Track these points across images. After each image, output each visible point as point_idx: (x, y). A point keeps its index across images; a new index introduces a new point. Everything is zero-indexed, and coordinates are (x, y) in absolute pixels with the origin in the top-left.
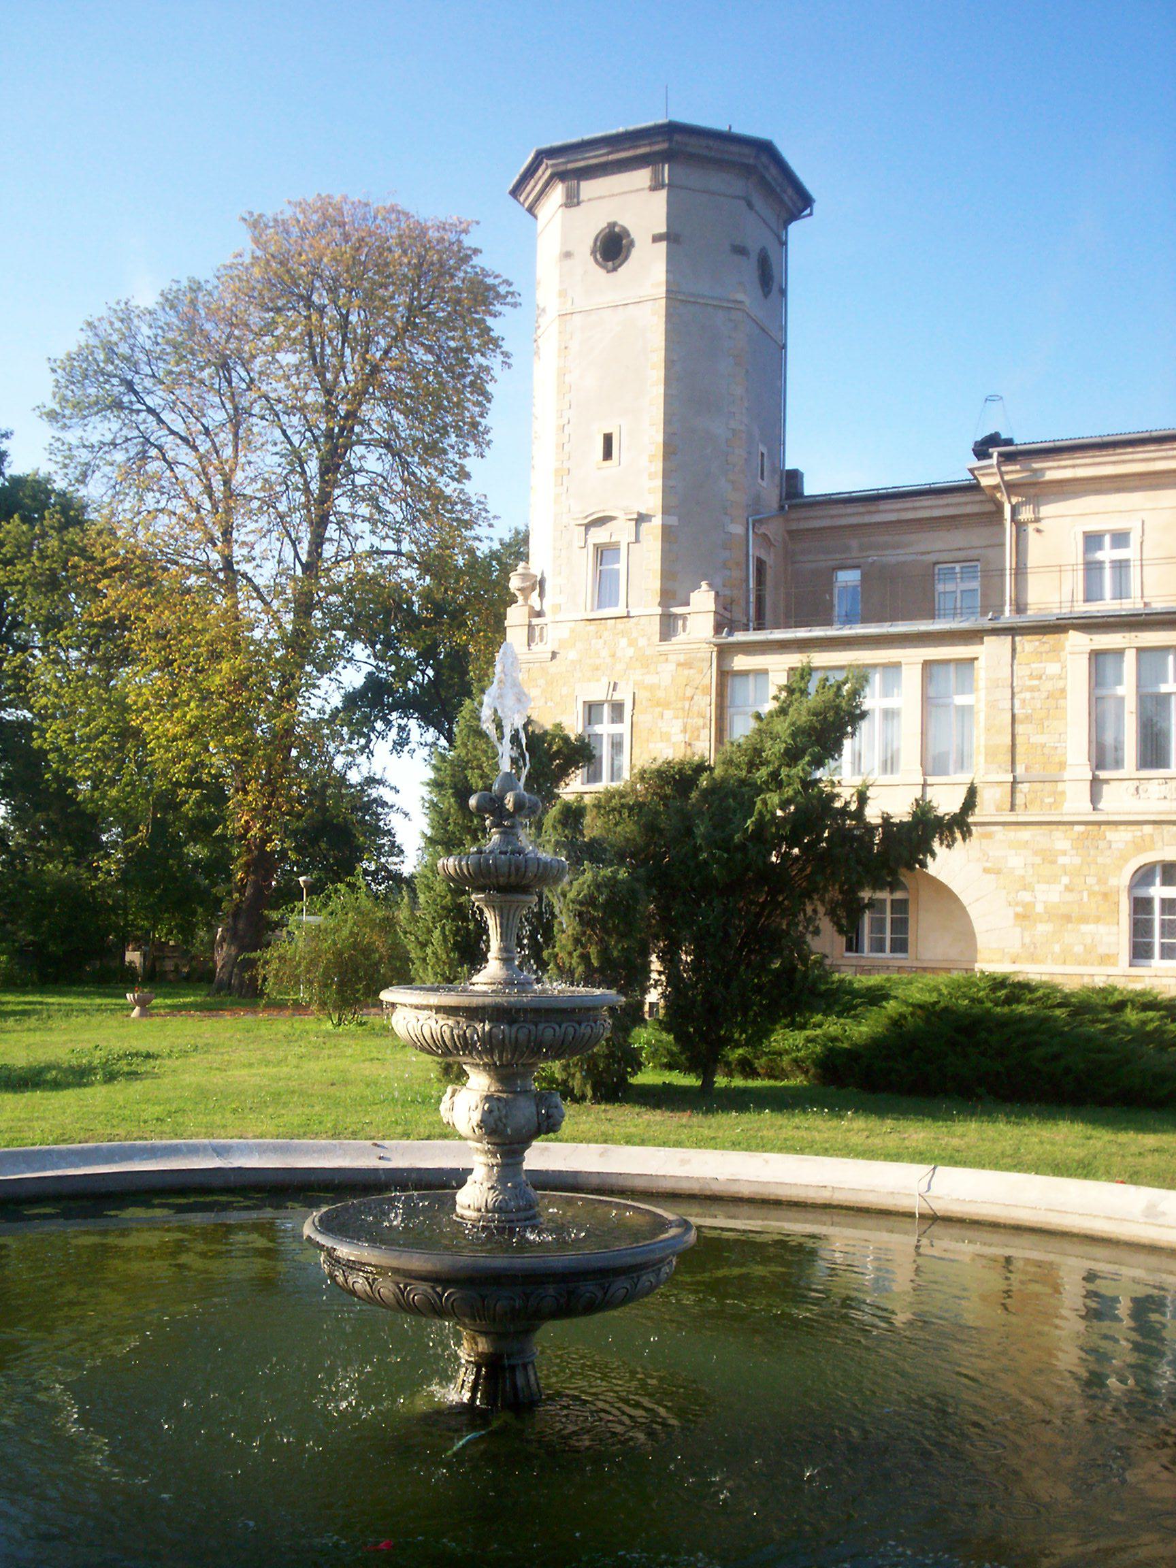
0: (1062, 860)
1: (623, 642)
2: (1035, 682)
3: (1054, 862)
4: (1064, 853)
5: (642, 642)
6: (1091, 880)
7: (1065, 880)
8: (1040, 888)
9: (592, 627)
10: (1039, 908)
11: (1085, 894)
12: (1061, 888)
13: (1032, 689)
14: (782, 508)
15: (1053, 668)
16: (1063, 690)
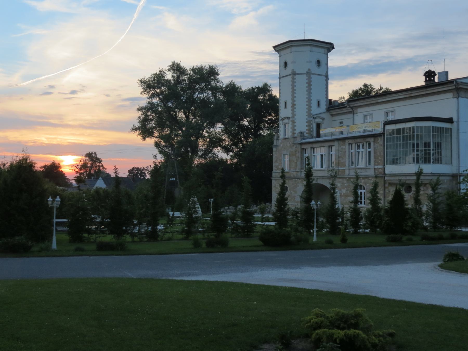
0: (346, 185)
1: (288, 143)
2: (342, 150)
3: (344, 185)
4: (345, 183)
5: (291, 143)
6: (349, 189)
7: (346, 189)
8: (342, 190)
9: (284, 140)
10: (342, 194)
11: (348, 191)
12: (345, 190)
13: (341, 151)
14: (327, 110)
15: (344, 147)
16: (345, 152)
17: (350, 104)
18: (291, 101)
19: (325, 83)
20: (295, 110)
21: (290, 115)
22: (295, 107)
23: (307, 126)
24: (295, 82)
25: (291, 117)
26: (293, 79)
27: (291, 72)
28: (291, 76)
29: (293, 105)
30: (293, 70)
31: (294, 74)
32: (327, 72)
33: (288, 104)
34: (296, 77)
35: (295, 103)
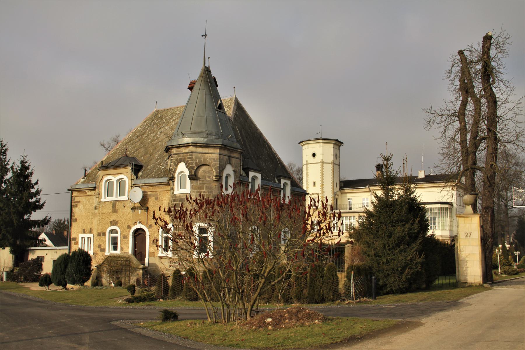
17: (370, 188)
18: (321, 182)
19: (338, 170)
20: (324, 189)
21: (320, 192)
22: (324, 186)
23: (332, 200)
24: (324, 169)
25: (320, 194)
26: (322, 166)
27: (320, 161)
28: (320, 164)
29: (322, 185)
30: (322, 160)
31: (323, 162)
32: (339, 163)
33: (316, 184)
34: (324, 165)
35: (324, 183)
